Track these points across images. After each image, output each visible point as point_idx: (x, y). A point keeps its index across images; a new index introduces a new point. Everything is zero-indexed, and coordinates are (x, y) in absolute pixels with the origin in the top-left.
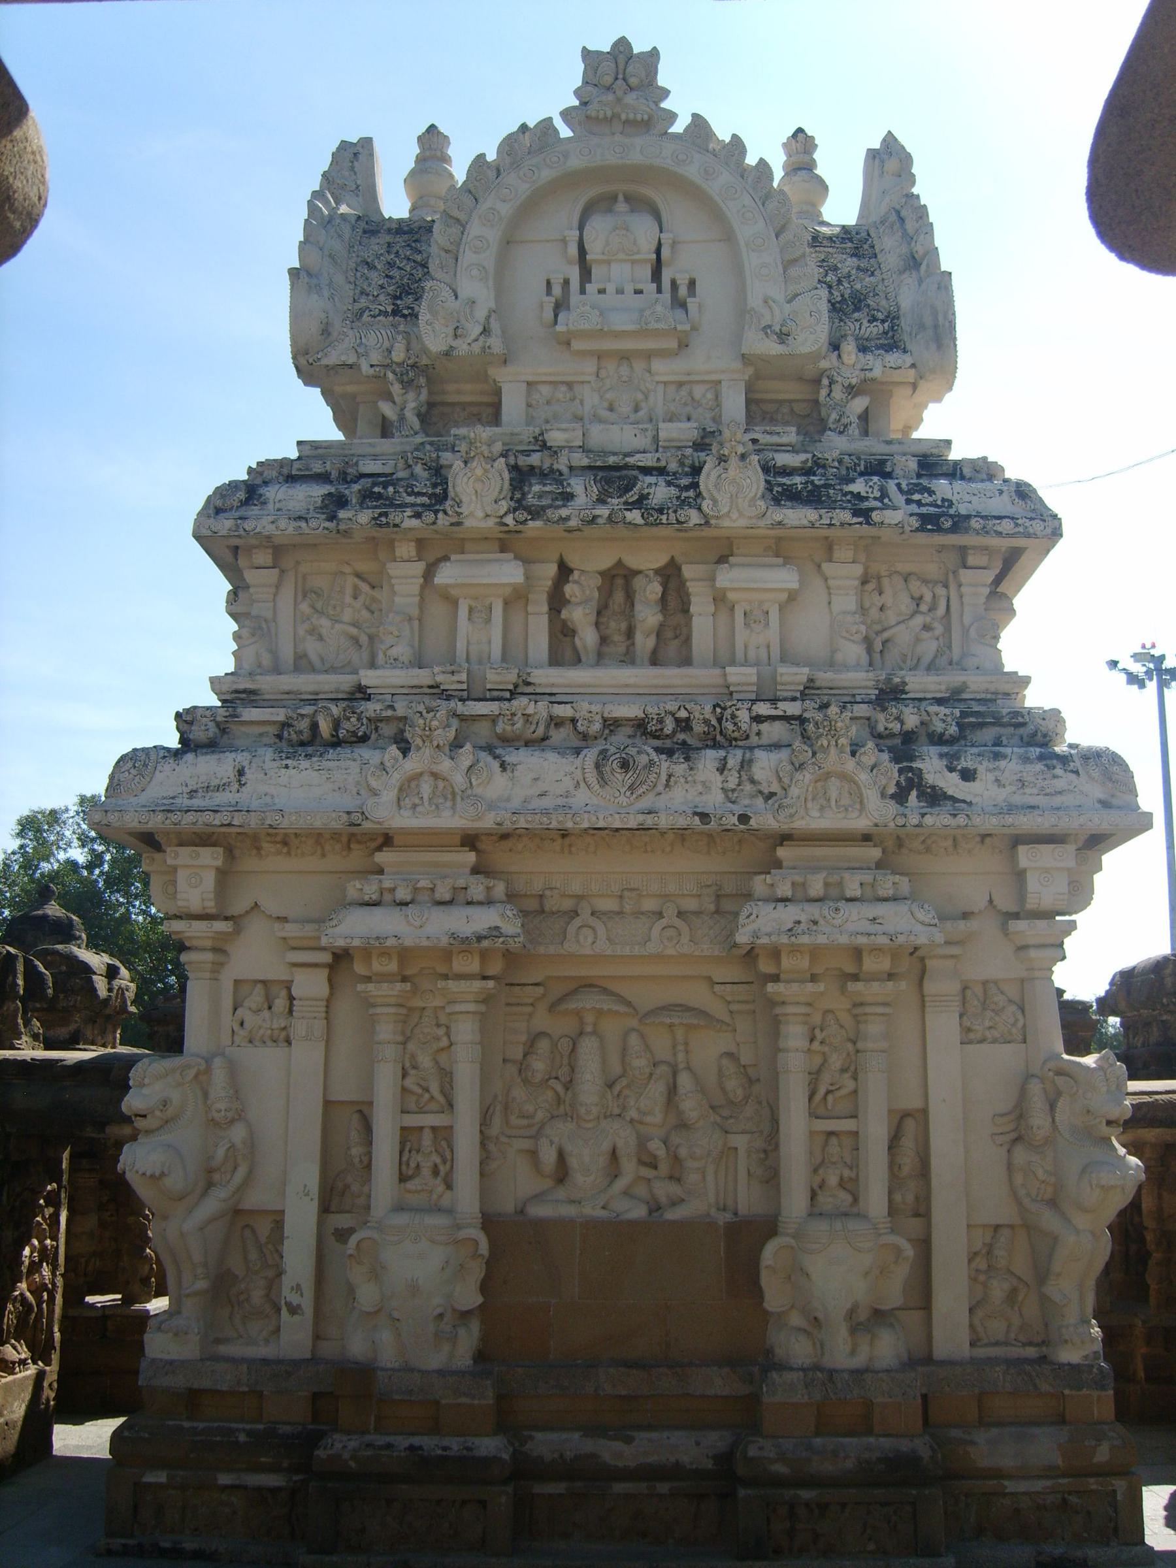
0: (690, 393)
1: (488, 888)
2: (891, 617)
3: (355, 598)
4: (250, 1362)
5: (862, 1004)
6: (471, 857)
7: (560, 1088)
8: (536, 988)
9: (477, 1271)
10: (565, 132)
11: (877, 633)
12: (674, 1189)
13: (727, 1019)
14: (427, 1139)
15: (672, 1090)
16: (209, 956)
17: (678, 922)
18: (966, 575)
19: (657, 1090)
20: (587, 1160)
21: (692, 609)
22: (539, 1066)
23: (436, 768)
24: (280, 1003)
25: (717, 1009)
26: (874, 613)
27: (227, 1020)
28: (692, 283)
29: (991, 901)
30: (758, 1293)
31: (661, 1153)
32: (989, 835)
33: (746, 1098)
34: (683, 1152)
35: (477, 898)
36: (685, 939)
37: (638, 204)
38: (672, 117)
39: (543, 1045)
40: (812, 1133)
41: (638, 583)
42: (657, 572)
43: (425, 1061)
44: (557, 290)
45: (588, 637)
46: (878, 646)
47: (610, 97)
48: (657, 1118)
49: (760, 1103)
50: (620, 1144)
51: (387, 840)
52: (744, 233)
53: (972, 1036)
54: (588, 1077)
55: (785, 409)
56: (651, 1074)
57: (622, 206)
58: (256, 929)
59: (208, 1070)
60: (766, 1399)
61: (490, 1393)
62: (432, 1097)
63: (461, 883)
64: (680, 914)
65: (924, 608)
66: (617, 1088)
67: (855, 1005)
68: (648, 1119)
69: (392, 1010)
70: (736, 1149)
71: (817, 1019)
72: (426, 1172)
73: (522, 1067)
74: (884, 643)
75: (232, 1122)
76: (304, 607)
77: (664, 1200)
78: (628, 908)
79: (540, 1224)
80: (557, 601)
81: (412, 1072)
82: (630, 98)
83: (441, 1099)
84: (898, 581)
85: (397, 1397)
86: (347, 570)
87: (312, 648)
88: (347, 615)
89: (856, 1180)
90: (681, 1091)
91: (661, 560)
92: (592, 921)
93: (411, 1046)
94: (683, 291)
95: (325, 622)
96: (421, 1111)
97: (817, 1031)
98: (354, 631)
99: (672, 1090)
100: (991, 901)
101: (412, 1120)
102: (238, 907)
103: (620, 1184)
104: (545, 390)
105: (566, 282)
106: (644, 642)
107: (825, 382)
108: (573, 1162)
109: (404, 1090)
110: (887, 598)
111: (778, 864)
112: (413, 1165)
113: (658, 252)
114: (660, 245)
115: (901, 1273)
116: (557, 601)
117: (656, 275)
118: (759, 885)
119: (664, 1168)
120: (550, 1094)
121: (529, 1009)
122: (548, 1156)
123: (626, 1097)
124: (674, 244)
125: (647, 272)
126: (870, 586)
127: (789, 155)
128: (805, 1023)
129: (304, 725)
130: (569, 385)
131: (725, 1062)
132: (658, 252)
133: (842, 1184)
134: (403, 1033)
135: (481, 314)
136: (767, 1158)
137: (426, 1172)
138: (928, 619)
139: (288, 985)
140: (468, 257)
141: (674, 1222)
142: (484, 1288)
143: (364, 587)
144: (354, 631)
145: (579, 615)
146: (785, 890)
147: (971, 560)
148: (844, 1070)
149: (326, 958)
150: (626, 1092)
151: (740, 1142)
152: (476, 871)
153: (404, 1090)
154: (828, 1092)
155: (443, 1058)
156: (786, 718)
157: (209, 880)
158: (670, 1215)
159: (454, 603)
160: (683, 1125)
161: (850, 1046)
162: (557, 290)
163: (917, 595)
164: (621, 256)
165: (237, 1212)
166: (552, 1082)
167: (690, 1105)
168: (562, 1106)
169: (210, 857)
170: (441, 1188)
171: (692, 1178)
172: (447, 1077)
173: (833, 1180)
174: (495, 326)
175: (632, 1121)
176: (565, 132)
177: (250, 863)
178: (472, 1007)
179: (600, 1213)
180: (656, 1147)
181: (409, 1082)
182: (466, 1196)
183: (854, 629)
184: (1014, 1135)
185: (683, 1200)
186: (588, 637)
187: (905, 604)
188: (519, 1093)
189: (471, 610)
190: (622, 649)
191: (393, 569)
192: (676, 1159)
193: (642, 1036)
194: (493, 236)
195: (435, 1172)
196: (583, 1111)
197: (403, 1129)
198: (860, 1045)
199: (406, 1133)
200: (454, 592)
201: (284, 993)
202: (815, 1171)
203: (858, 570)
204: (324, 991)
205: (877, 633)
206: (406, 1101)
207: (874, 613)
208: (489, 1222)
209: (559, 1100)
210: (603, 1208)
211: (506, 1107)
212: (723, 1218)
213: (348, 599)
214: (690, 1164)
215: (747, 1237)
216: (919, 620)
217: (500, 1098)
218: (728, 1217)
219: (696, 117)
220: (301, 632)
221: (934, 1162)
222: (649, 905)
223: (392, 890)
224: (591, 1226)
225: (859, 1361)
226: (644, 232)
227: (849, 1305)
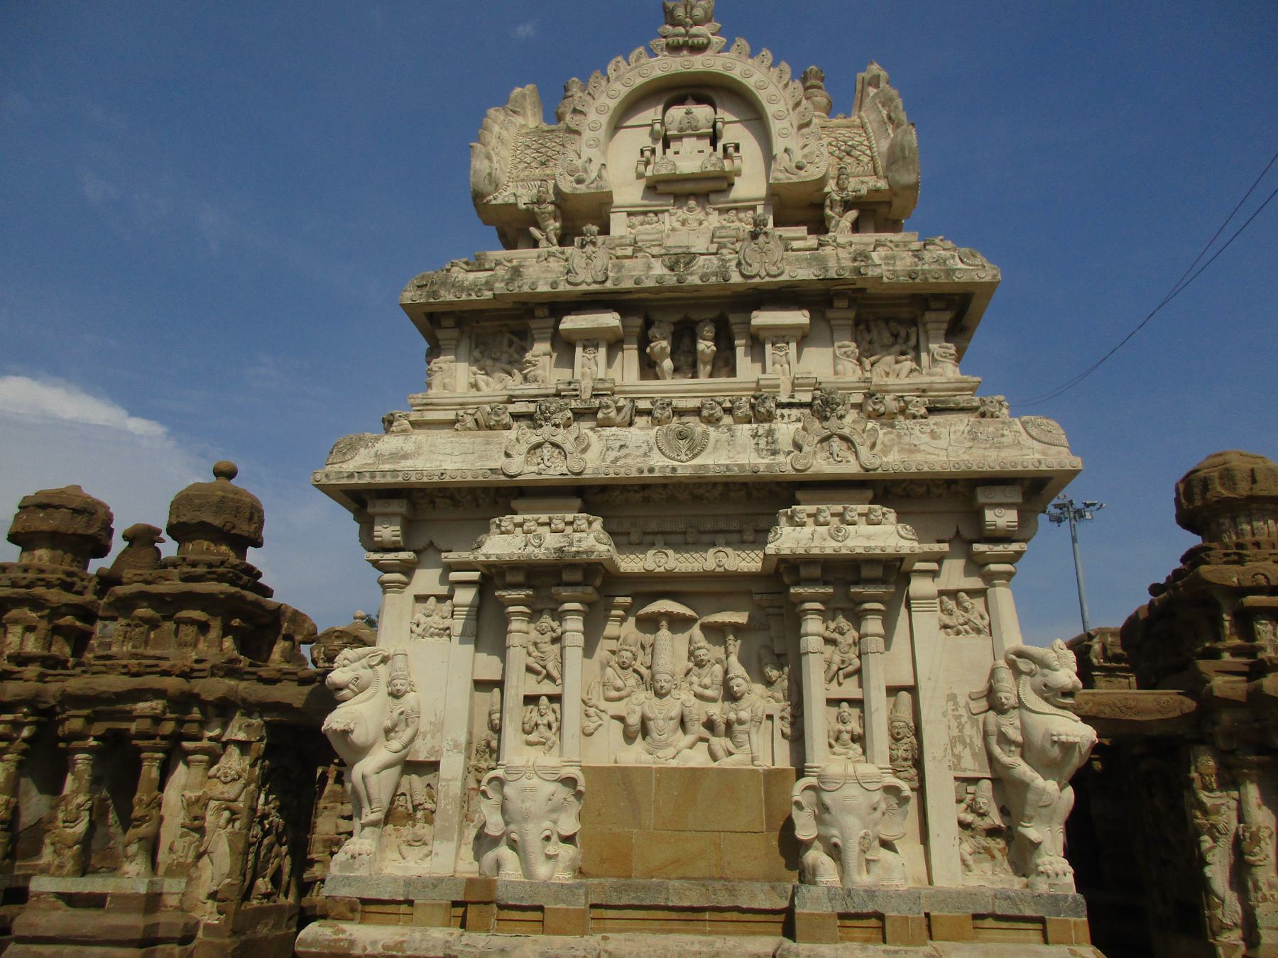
29: (958, 532)
44: (647, 154)
65: (900, 341)
94: (731, 150)
107: (828, 202)
113: (714, 126)
117: (714, 144)
126: (862, 327)
132: (714, 126)
143: (515, 339)
154: (840, 669)
158: (726, 763)
162: (647, 154)
164: (689, 132)
169: (399, 507)
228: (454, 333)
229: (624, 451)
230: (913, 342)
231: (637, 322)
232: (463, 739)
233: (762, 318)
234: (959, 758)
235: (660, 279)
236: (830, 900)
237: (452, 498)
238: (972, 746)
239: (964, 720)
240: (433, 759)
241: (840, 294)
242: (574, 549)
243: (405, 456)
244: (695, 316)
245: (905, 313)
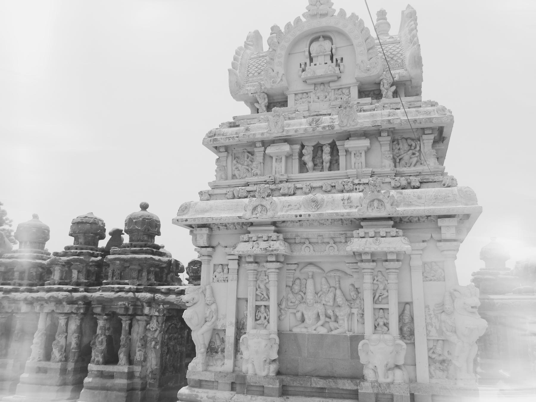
0: (342, 91)
1: (278, 237)
2: (402, 151)
3: (248, 158)
4: (215, 372)
5: (388, 269)
6: (273, 228)
7: (303, 294)
9: (276, 348)
10: (304, 20)
11: (398, 157)
12: (336, 325)
13: (351, 274)
14: (263, 309)
15: (335, 296)
16: (206, 258)
17: (334, 245)
18: (424, 137)
19: (331, 295)
20: (310, 316)
21: (339, 154)
22: (296, 288)
23: (263, 203)
24: (226, 270)
25: (349, 271)
26: (396, 151)
27: (212, 276)
28: (342, 59)
29: (432, 237)
30: (358, 358)
32: (430, 216)
34: (338, 314)
35: (274, 239)
36: (336, 250)
37: (326, 38)
38: (334, 11)
39: (298, 282)
40: (374, 309)
41: (324, 147)
42: (329, 144)
43: (262, 286)
44: (303, 66)
45: (310, 165)
46: (398, 160)
47: (315, 7)
48: (331, 303)
50: (320, 311)
51: (252, 224)
52: (355, 42)
53: (427, 279)
55: (372, 93)
57: (321, 39)
58: (220, 250)
59: (205, 289)
60: (359, 391)
61: (278, 384)
62: (264, 297)
63: (270, 235)
64: (335, 243)
65: (413, 148)
66: (319, 295)
67: (387, 269)
68: (328, 304)
69: (252, 271)
71: (376, 273)
72: (262, 318)
73: (291, 288)
74: (400, 160)
75: (212, 304)
76: (234, 162)
77: (333, 328)
78: (320, 242)
79: (295, 335)
80: (301, 155)
81: (258, 289)
82: (321, 7)
83: (267, 297)
84: (404, 141)
85: (252, 384)
86: (245, 151)
87: (236, 173)
88: (246, 163)
89: (388, 323)
91: (330, 141)
92: (309, 245)
93: (258, 282)
94: (339, 61)
95: (240, 166)
96: (261, 300)
97: (375, 277)
98: (247, 167)
100: (432, 237)
101: (259, 303)
102: (214, 244)
103: (320, 323)
104: (300, 96)
105: (306, 63)
106: (326, 165)
107: (382, 83)
108: (306, 316)
109: (257, 295)
110: (401, 146)
111: (362, 227)
112: (259, 316)
114: (332, 49)
115: (403, 354)
116: (301, 155)
118: (355, 233)
121: (293, 271)
122: (299, 315)
124: (336, 48)
125: (329, 58)
126: (395, 143)
127: (378, 17)
128: (371, 275)
129: (231, 193)
130: (307, 93)
131: (351, 287)
133: (385, 325)
134: (256, 278)
135: (280, 75)
137: (262, 318)
138: (414, 151)
139: (228, 265)
140: (276, 60)
141: (334, 335)
142: (279, 353)
143: (250, 155)
144: (247, 167)
145: (307, 158)
146: (362, 234)
147: (426, 132)
148: (384, 289)
149: (237, 257)
151: (355, 311)
152: (275, 231)
153: (257, 295)
155: (267, 286)
156: (364, 184)
157: (205, 237)
159: (271, 157)
161: (386, 282)
162: (303, 66)
163: (410, 144)
164: (321, 54)
165: (214, 329)
166: (301, 293)
167: (340, 300)
169: (205, 231)
170: (267, 323)
171: (341, 322)
172: (268, 289)
173: (381, 324)
174: (284, 79)
176: (304, 20)
177: (216, 232)
178: (274, 270)
180: (330, 312)
181: (258, 292)
182: (273, 326)
183: (388, 156)
184: (441, 311)
186: (310, 165)
187: (406, 147)
188: (291, 296)
189: (276, 159)
190: (321, 167)
191: (256, 150)
192: (336, 317)
193: (326, 279)
194: (283, 53)
195: (265, 318)
196: (308, 301)
197: (256, 306)
198: (389, 282)
199: (258, 307)
200: (271, 155)
201: (226, 267)
202: (376, 320)
203: (389, 138)
204: (237, 267)
205: (398, 157)
206: (257, 297)
207: (396, 151)
208: (280, 334)
209: (303, 298)
210: (315, 330)
211: (287, 300)
212: (349, 334)
213: (246, 159)
214: (340, 317)
215: (356, 339)
216: (411, 152)
219: (341, 9)
220: (234, 168)
221: (415, 318)
222: (326, 240)
223: (252, 238)
225: (389, 380)
226: (327, 45)
227: (386, 363)
228: (225, 154)
229: (290, 207)
230: (418, 148)
231: (297, 147)
232: (234, 321)
233: (350, 144)
234: (430, 331)
235: (306, 130)
236: (372, 388)
237: (226, 226)
238: (435, 327)
239: (432, 316)
240: (223, 328)
241: (383, 130)
242: (271, 249)
243: (207, 211)
244: (322, 142)
245: (414, 136)
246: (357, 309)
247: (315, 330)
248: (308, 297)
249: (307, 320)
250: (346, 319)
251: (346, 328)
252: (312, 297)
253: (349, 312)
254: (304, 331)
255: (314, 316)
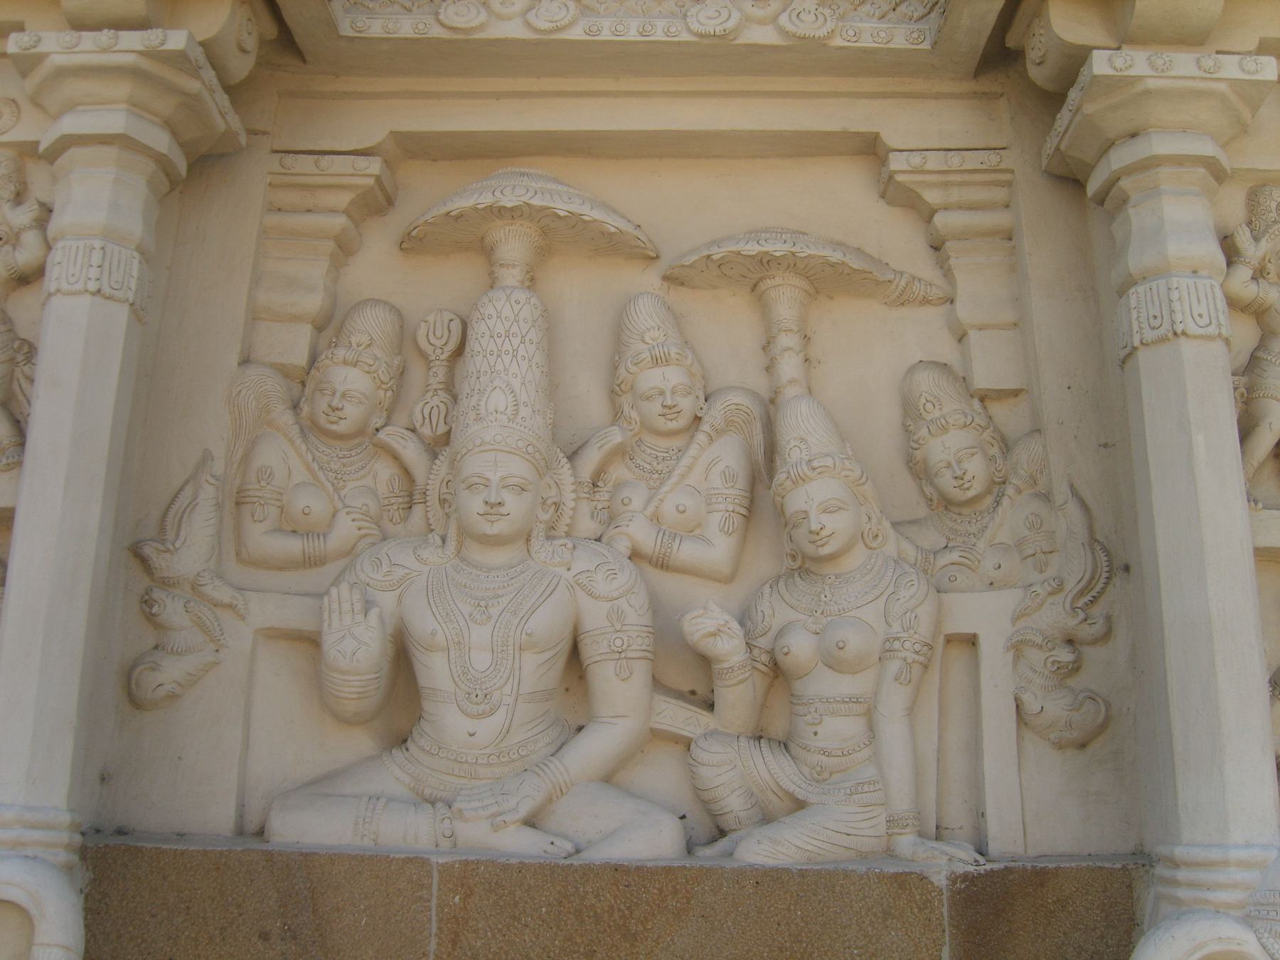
7: (412, 452)
8: (362, 162)
15: (764, 466)
19: (718, 463)
20: (484, 652)
22: (352, 382)
31: (729, 647)
33: (997, 486)
34: (800, 647)
48: (716, 549)
49: (1046, 497)
50: (595, 617)
54: (499, 400)
56: (698, 419)
66: (591, 459)
68: (687, 552)
70: (971, 641)
73: (302, 381)
77: (734, 804)
90: (793, 453)
99: (764, 466)
103: (598, 745)
108: (435, 671)
119: (737, 698)
120: (385, 471)
123: (619, 486)
131: (926, 382)
136: (1076, 668)
141: (772, 878)
150: (619, 472)
151: (987, 613)
158: (760, 850)
160: (804, 564)
168: (418, 510)
171: (837, 730)
175: (635, 555)
179: (520, 843)
180: (711, 623)
185: (800, 805)
188: (281, 457)
196: (473, 504)
210: (531, 822)
212: (945, 863)
217: (218, 467)
218: (963, 859)
224: (482, 880)
246: (1008, 600)
247: (531, 822)
248: (474, 465)
249: (451, 722)
250: (894, 701)
251: (902, 802)
252: (518, 468)
253: (924, 629)
254: (407, 831)
255: (539, 669)
